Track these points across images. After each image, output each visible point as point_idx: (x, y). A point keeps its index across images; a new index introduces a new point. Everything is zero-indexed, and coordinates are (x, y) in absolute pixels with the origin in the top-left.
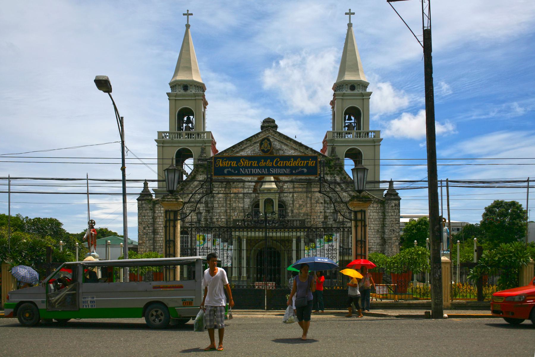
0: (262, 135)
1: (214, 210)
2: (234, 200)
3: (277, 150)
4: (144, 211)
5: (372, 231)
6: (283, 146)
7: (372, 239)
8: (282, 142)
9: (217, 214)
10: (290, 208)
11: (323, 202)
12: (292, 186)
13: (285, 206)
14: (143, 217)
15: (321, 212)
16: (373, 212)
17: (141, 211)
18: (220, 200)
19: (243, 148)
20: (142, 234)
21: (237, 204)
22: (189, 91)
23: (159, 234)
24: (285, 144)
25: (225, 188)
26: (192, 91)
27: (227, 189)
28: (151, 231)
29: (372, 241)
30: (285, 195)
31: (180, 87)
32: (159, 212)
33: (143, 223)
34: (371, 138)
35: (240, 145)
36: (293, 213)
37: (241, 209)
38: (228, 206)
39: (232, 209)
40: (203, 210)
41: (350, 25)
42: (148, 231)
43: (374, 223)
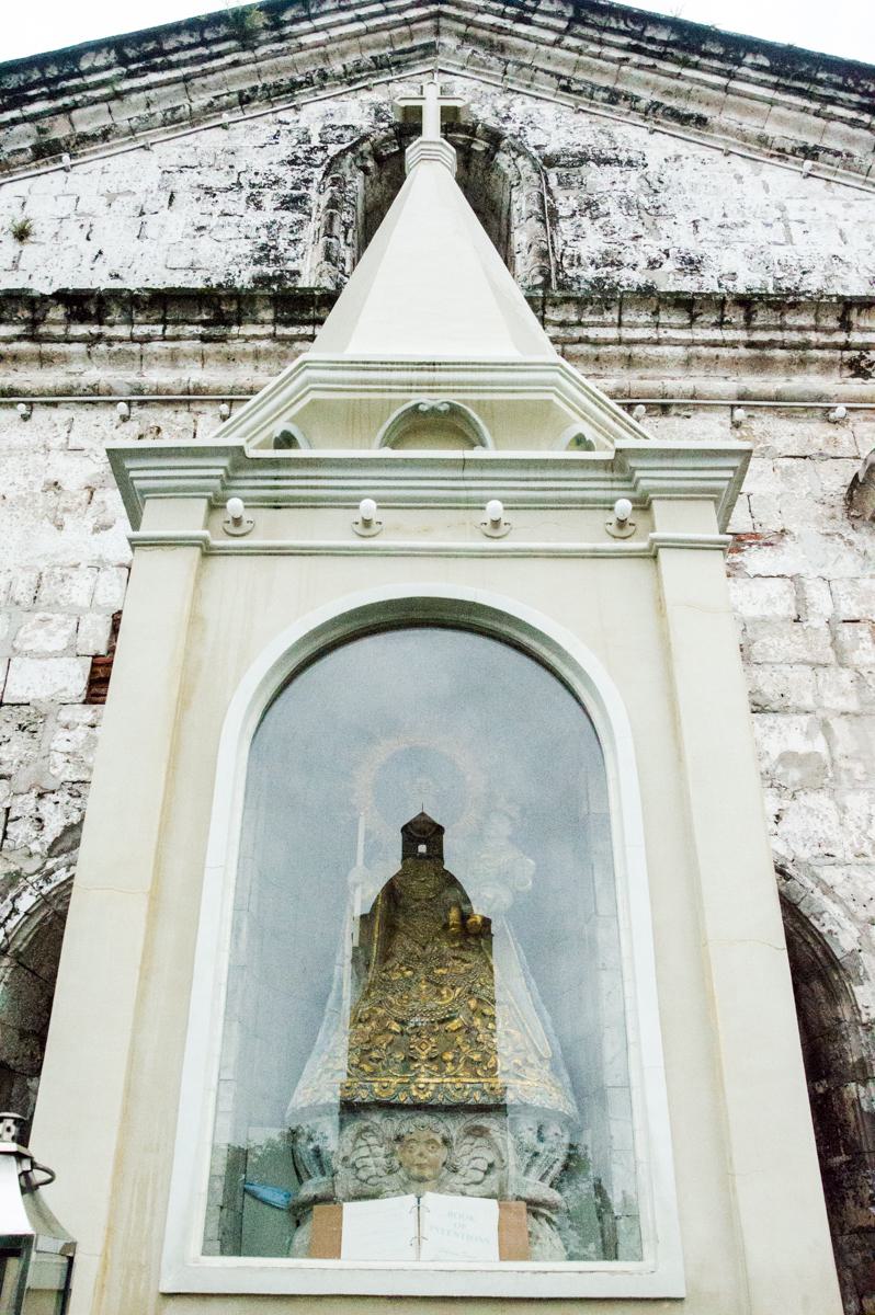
3: (550, 161)
6: (631, 135)
8: (614, 97)
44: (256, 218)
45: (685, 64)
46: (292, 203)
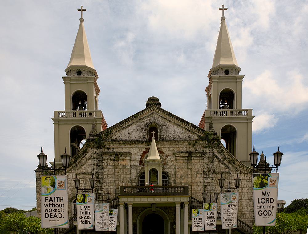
0: (147, 111)
5: (246, 198)
6: (166, 122)
7: (246, 206)
8: (165, 119)
9: (107, 184)
10: (172, 179)
11: (202, 173)
12: (174, 159)
13: (168, 176)
15: (201, 182)
16: (246, 182)
19: (129, 124)
21: (125, 175)
22: (82, 76)
24: (168, 120)
25: (114, 160)
26: (84, 75)
27: (115, 162)
29: (246, 208)
30: (168, 167)
31: (74, 72)
34: (244, 115)
35: (127, 121)
36: (175, 183)
37: (128, 179)
38: (117, 177)
39: (120, 180)
41: (223, 19)
43: (247, 191)
44: (143, 132)
45: (170, 116)
46: (145, 130)
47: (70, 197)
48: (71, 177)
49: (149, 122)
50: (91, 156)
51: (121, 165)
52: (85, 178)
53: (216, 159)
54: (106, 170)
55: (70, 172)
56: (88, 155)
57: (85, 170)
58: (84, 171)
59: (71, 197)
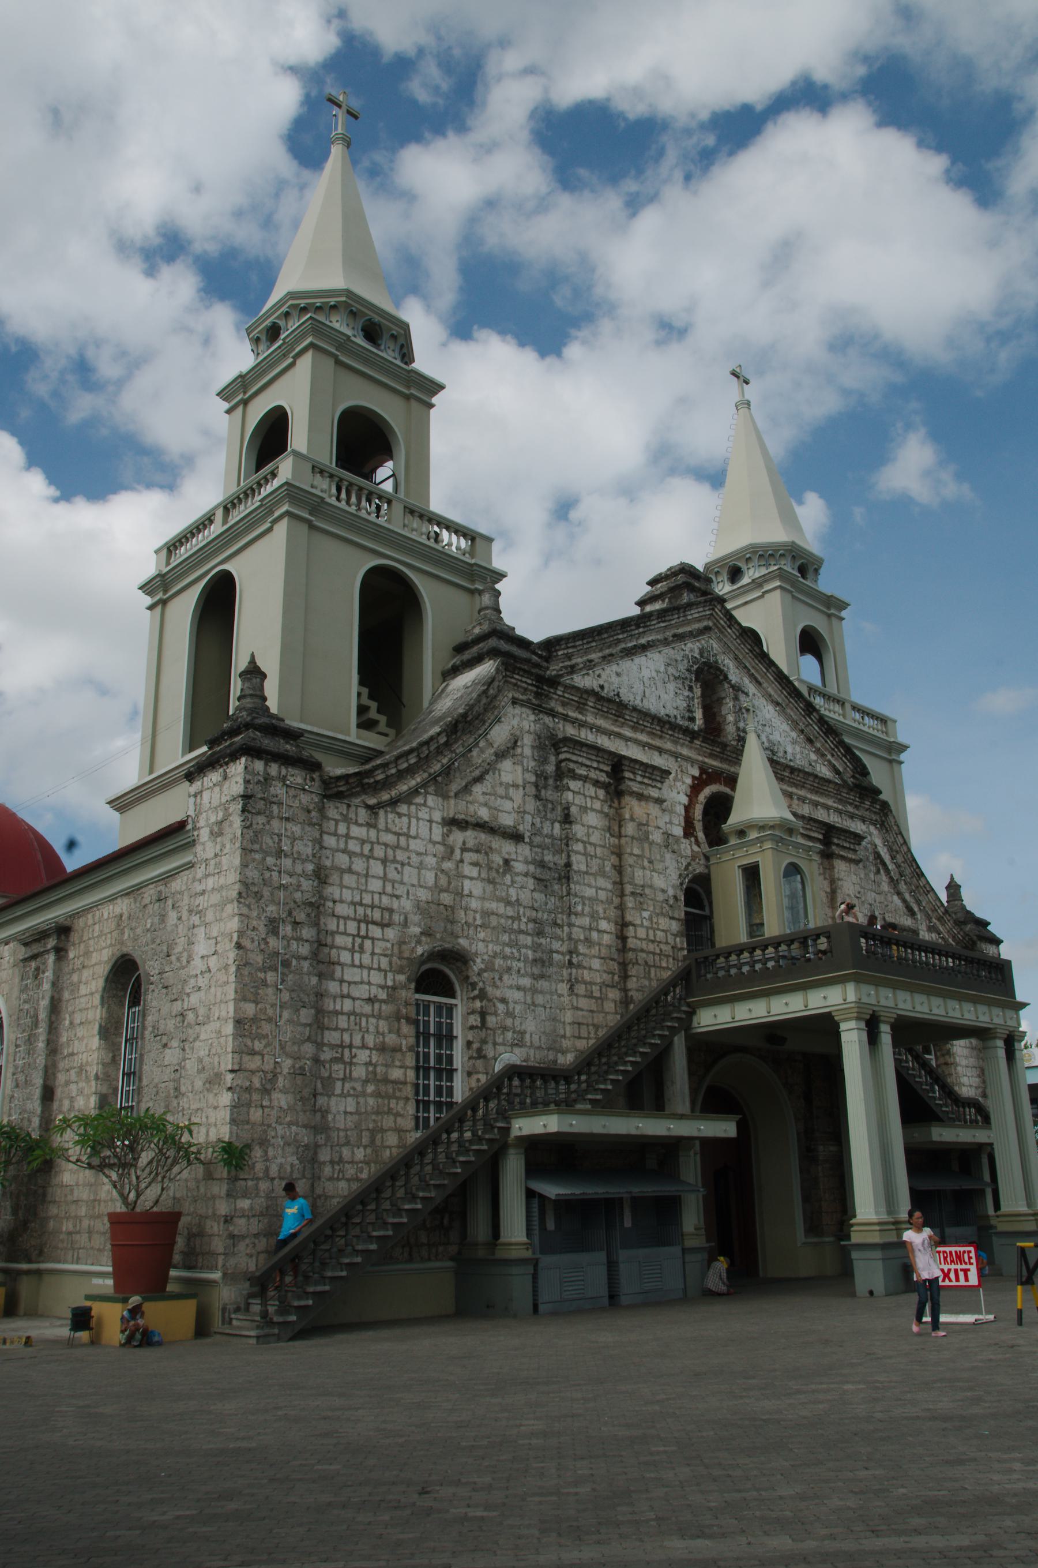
1: (572, 886)
2: (636, 851)
4: (275, 824)
6: (746, 680)
14: (270, 861)
17: (261, 820)
18: (594, 839)
19: (643, 641)
20: (258, 959)
21: (648, 872)
23: (338, 974)
28: (305, 950)
32: (342, 846)
33: (266, 892)
39: (633, 893)
40: (526, 875)
42: (294, 945)
46: (691, 689)
47: (413, 950)
48: (424, 830)
49: (698, 657)
50: (516, 742)
51: (632, 819)
52: (486, 854)
53: (882, 871)
54: (579, 830)
55: (419, 800)
56: (499, 734)
57: (486, 805)
58: (484, 814)
59: (420, 950)
